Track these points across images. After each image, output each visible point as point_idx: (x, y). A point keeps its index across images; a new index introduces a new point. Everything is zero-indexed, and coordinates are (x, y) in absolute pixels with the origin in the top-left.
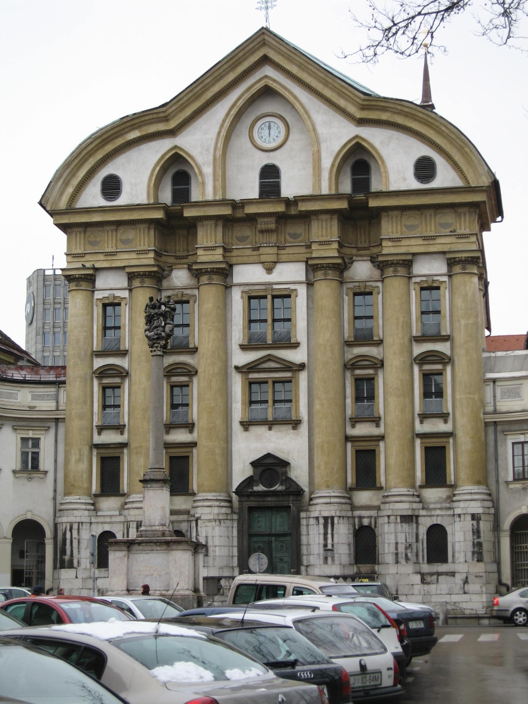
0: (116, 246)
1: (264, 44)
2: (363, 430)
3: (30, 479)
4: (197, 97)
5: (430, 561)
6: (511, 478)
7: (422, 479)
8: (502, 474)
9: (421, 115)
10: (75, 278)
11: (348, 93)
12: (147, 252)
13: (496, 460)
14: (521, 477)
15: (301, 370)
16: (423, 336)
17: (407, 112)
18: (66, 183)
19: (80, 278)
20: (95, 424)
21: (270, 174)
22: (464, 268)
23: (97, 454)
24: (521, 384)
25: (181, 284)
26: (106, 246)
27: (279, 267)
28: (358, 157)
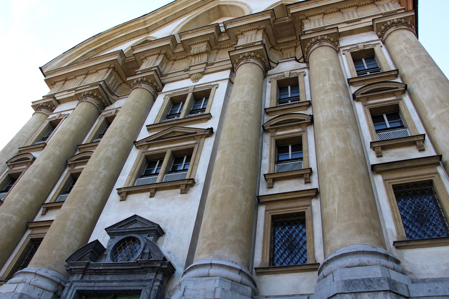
19: (42, 106)
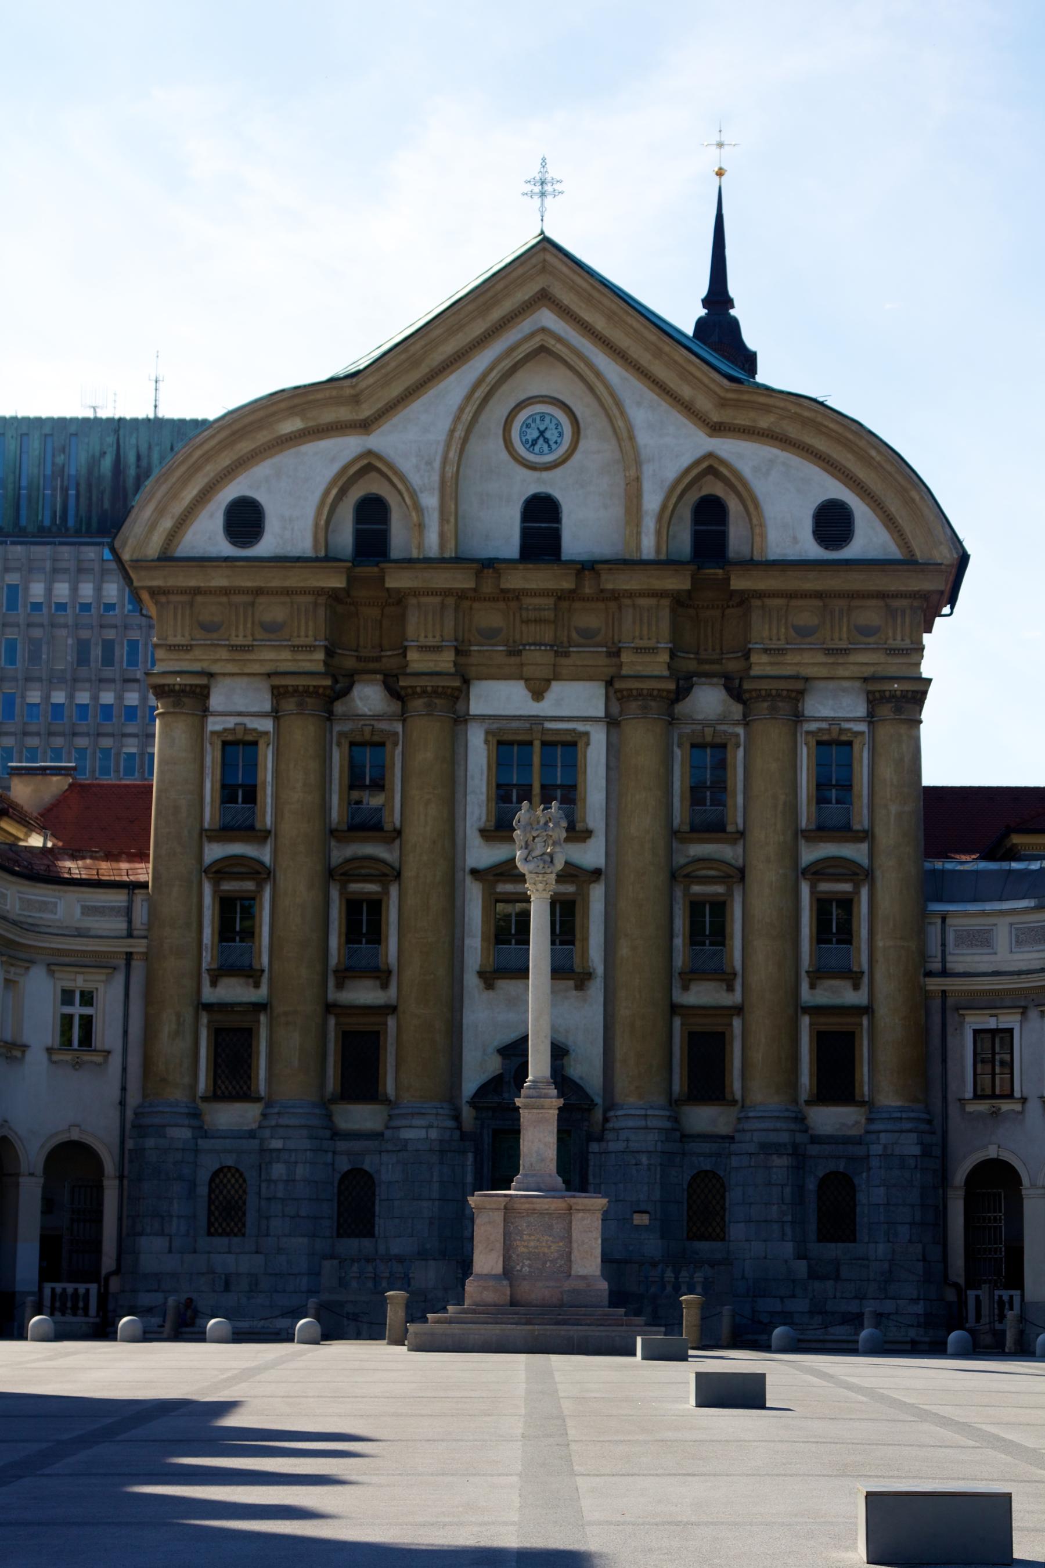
0: (253, 635)
1: (544, 268)
2: (703, 994)
3: (77, 1065)
4: (415, 362)
5: (825, 1236)
6: (969, 1094)
7: (811, 1089)
8: (953, 1086)
9: (832, 425)
10: (173, 691)
11: (698, 374)
12: (311, 648)
13: (944, 1061)
14: (989, 1092)
15: (594, 881)
16: (820, 828)
17: (807, 418)
18: (161, 511)
19: (183, 691)
20: (204, 966)
21: (541, 515)
22: (898, 710)
23: (209, 1022)
24: (995, 925)
25: (370, 710)
26: (234, 633)
27: (557, 688)
28: (705, 491)
